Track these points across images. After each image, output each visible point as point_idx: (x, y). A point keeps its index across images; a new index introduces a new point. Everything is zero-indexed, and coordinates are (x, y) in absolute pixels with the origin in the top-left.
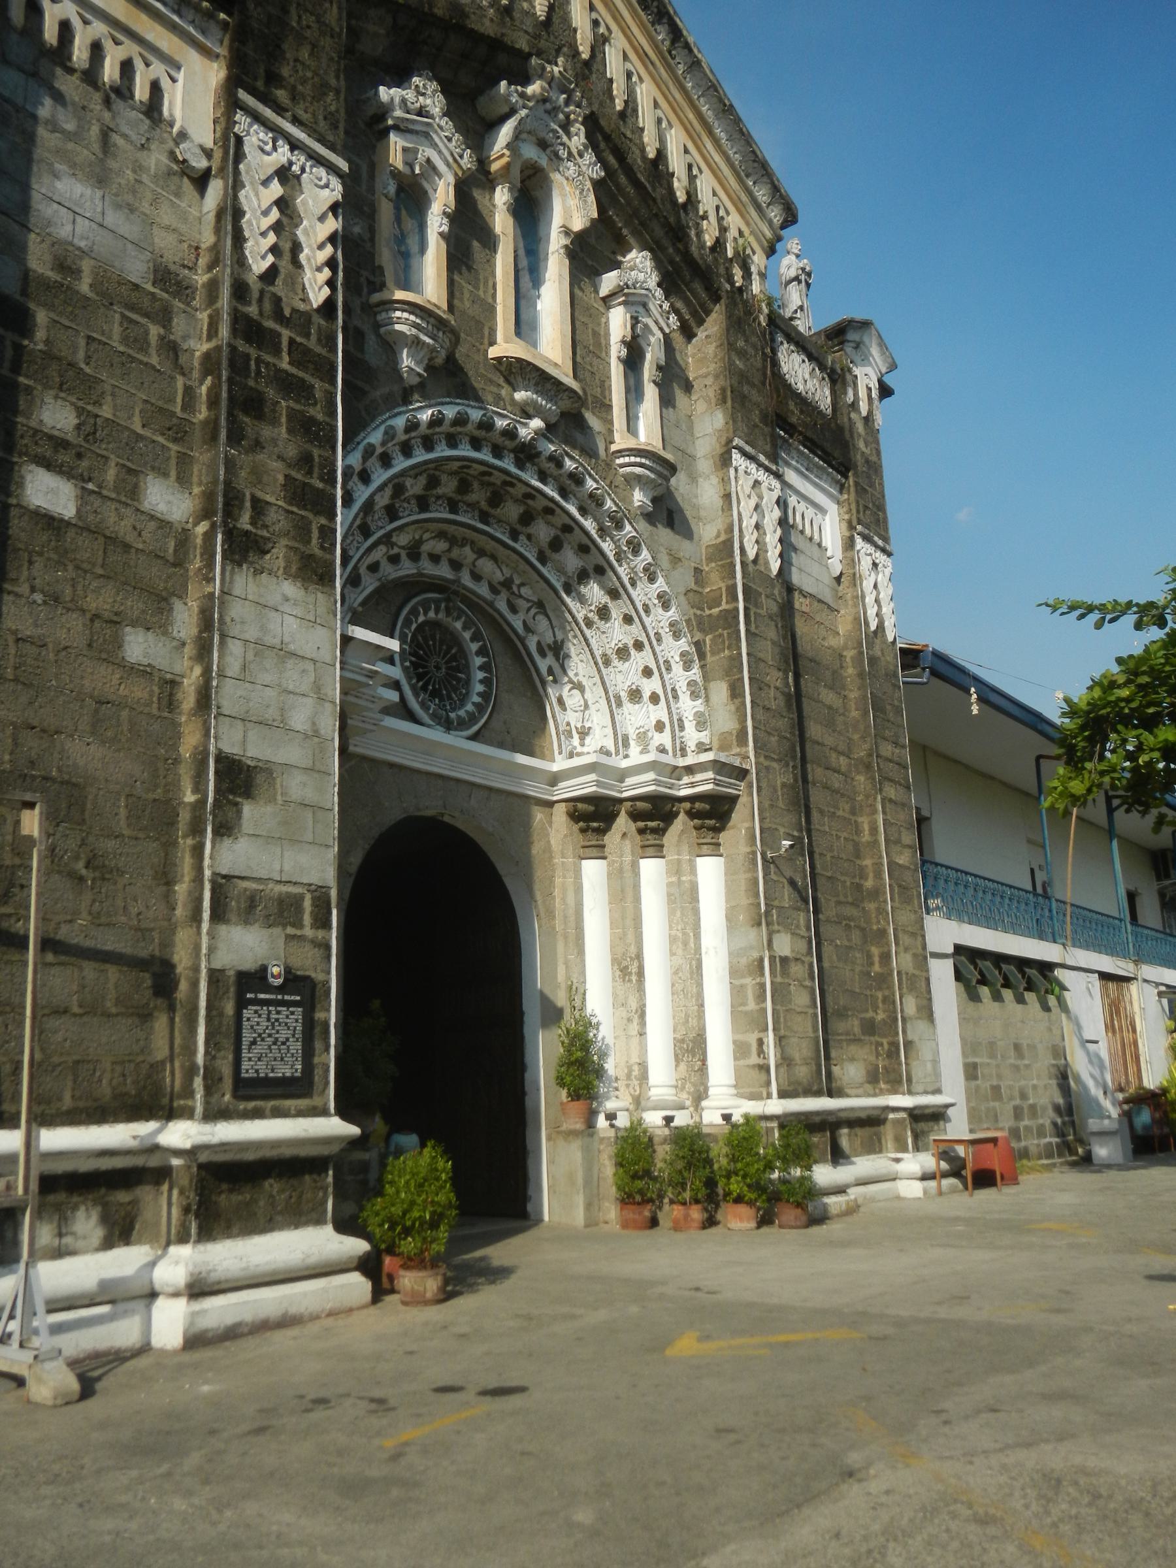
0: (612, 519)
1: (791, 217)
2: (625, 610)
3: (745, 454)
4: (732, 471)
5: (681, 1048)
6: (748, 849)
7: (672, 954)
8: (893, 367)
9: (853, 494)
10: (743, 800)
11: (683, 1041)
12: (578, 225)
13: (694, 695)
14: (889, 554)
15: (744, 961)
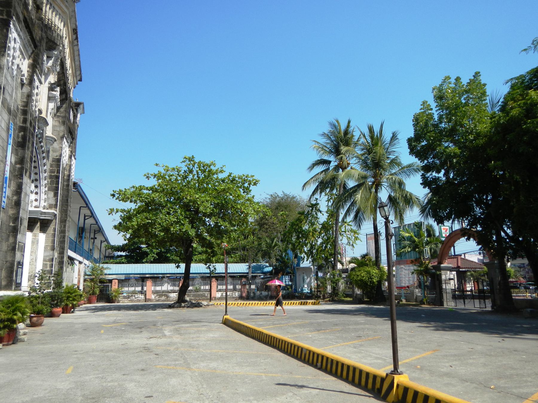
0: (43, 151)
1: (81, 80)
2: (36, 171)
3: (66, 139)
4: (63, 142)
5: (30, 278)
6: (53, 233)
7: (31, 255)
8: (84, 113)
9: (74, 145)
10: (54, 221)
11: (31, 276)
12: (53, 82)
13: (45, 194)
14: (75, 159)
15: (48, 258)
